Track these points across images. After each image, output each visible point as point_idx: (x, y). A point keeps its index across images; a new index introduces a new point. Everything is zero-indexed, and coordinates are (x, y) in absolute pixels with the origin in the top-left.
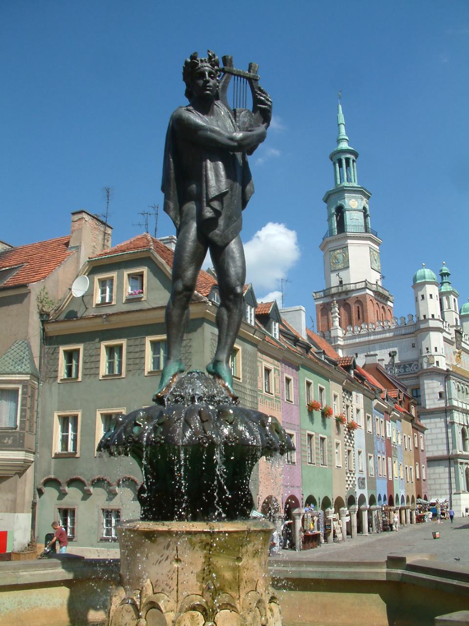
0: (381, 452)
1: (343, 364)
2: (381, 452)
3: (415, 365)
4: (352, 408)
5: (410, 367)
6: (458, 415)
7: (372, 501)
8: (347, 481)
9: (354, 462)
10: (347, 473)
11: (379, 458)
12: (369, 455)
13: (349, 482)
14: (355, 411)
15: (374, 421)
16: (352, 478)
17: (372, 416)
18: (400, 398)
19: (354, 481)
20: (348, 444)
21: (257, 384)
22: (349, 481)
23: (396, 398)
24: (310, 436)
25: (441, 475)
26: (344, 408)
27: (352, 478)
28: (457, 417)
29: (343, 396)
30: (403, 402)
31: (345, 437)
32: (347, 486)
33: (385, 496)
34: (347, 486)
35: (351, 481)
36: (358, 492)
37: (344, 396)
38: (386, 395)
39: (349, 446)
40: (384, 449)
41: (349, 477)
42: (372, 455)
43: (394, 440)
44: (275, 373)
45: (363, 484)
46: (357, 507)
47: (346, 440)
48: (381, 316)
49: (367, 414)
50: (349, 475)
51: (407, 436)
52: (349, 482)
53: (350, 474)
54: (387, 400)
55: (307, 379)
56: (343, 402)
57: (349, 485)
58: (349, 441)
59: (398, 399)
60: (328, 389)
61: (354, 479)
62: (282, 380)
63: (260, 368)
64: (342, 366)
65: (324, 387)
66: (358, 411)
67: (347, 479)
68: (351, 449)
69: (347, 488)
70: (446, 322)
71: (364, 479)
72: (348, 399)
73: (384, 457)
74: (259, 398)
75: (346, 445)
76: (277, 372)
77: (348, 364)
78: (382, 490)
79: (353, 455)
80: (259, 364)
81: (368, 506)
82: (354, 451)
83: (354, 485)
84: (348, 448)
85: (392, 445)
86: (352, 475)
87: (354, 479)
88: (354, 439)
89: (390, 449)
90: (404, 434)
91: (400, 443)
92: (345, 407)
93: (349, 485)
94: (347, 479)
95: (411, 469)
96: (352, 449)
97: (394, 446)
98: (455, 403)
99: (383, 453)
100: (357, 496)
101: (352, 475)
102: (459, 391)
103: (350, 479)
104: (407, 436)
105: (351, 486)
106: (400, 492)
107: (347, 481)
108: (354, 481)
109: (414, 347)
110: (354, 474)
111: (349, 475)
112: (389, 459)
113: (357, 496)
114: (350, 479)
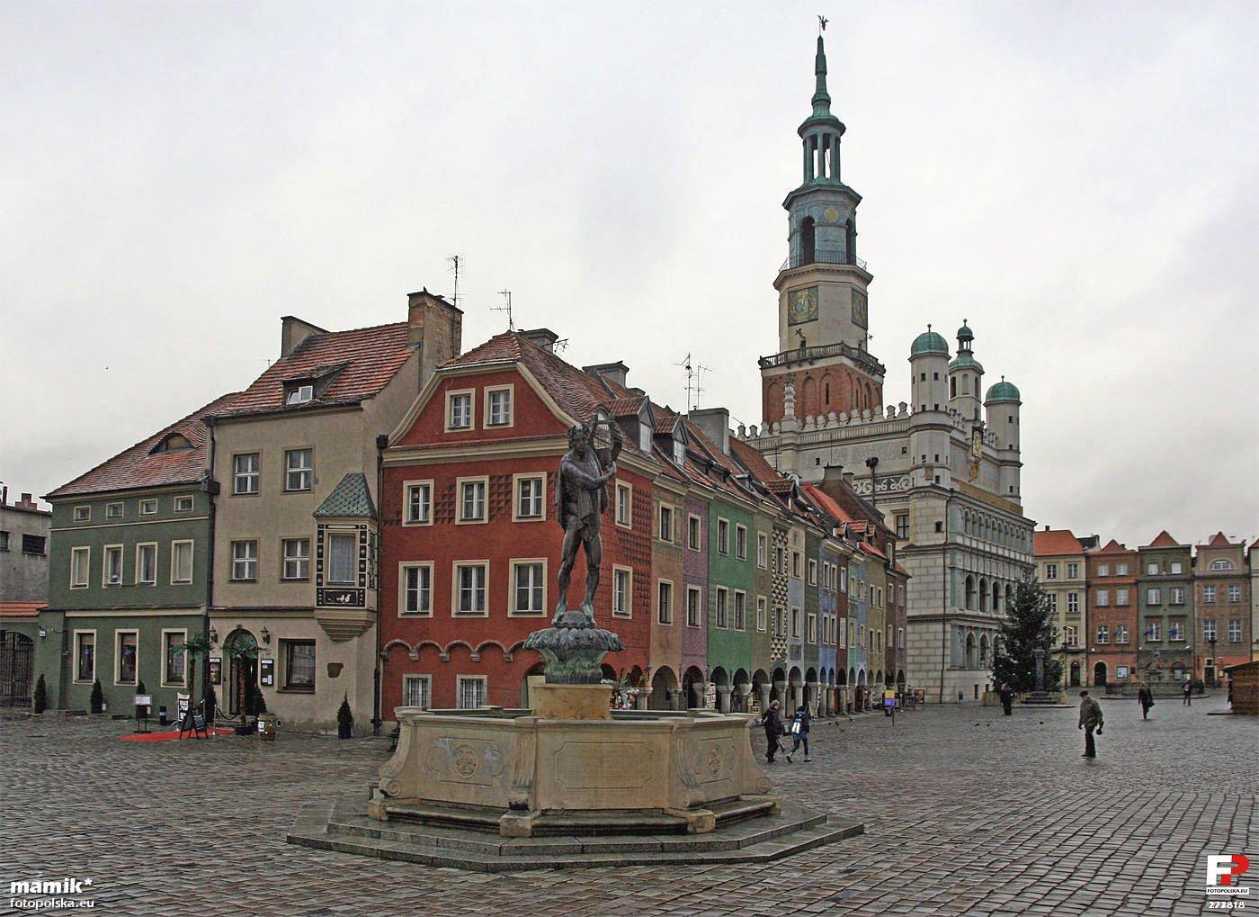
0: (830, 611)
6: (962, 558)
11: (826, 618)
17: (818, 562)
18: (868, 533)
23: (862, 534)
28: (960, 560)
42: (815, 615)
45: (798, 652)
46: (787, 683)
60: (753, 529)
70: (959, 415)
71: (799, 647)
73: (834, 617)
75: (774, 602)
84: (777, 606)
98: (959, 540)
99: (833, 612)
102: (967, 520)
112: (843, 621)
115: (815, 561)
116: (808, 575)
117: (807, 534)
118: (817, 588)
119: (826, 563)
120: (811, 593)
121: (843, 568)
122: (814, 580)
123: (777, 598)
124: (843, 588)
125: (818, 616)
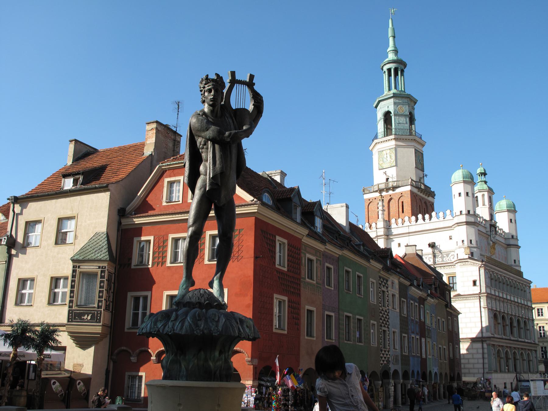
0: (415, 333)
1: (381, 255)
2: (415, 333)
3: (452, 255)
4: (388, 293)
5: (448, 256)
7: (406, 375)
8: (382, 357)
9: (389, 341)
10: (382, 351)
11: (413, 337)
12: (403, 335)
13: (383, 359)
14: (390, 296)
15: (409, 305)
16: (387, 355)
19: (389, 358)
20: (383, 325)
21: (300, 272)
22: (382, 356)
23: (431, 285)
24: (348, 317)
25: (472, 357)
26: (380, 293)
27: (387, 355)
29: (379, 283)
30: (438, 289)
31: (381, 319)
32: (382, 362)
33: (418, 372)
34: (382, 362)
35: (385, 358)
36: (392, 367)
37: (380, 283)
38: (421, 282)
39: (384, 326)
40: (418, 329)
41: (383, 354)
42: (406, 335)
44: (317, 263)
47: (381, 321)
48: (423, 210)
49: (402, 299)
50: (383, 352)
52: (383, 359)
53: (385, 351)
54: (423, 287)
55: (346, 268)
56: (380, 288)
57: (383, 361)
58: (384, 322)
59: (433, 286)
61: (388, 356)
62: (323, 268)
63: (303, 258)
64: (380, 256)
65: (362, 275)
66: (393, 296)
67: (382, 355)
68: (386, 329)
69: (382, 364)
72: (384, 286)
74: (302, 284)
75: (381, 326)
76: (319, 262)
77: (386, 254)
78: (414, 366)
79: (387, 334)
80: (302, 255)
81: (402, 381)
82: (388, 331)
83: (388, 361)
84: (383, 328)
86: (387, 352)
87: (388, 356)
88: (389, 320)
89: (423, 330)
90: (439, 318)
92: (382, 292)
93: (383, 361)
94: (382, 355)
96: (386, 329)
97: (428, 328)
100: (392, 371)
101: (387, 352)
103: (385, 356)
104: (441, 320)
105: (385, 362)
106: (434, 369)
107: (382, 357)
108: (389, 358)
109: (451, 239)
110: (388, 352)
111: (383, 352)
113: (392, 371)
114: (385, 356)
115: (405, 300)
116: (401, 309)
117: (400, 284)
118: (407, 318)
119: (412, 302)
120: (404, 322)
121: (422, 306)
122: (405, 312)
123: (383, 323)
124: (422, 318)
125: (408, 336)
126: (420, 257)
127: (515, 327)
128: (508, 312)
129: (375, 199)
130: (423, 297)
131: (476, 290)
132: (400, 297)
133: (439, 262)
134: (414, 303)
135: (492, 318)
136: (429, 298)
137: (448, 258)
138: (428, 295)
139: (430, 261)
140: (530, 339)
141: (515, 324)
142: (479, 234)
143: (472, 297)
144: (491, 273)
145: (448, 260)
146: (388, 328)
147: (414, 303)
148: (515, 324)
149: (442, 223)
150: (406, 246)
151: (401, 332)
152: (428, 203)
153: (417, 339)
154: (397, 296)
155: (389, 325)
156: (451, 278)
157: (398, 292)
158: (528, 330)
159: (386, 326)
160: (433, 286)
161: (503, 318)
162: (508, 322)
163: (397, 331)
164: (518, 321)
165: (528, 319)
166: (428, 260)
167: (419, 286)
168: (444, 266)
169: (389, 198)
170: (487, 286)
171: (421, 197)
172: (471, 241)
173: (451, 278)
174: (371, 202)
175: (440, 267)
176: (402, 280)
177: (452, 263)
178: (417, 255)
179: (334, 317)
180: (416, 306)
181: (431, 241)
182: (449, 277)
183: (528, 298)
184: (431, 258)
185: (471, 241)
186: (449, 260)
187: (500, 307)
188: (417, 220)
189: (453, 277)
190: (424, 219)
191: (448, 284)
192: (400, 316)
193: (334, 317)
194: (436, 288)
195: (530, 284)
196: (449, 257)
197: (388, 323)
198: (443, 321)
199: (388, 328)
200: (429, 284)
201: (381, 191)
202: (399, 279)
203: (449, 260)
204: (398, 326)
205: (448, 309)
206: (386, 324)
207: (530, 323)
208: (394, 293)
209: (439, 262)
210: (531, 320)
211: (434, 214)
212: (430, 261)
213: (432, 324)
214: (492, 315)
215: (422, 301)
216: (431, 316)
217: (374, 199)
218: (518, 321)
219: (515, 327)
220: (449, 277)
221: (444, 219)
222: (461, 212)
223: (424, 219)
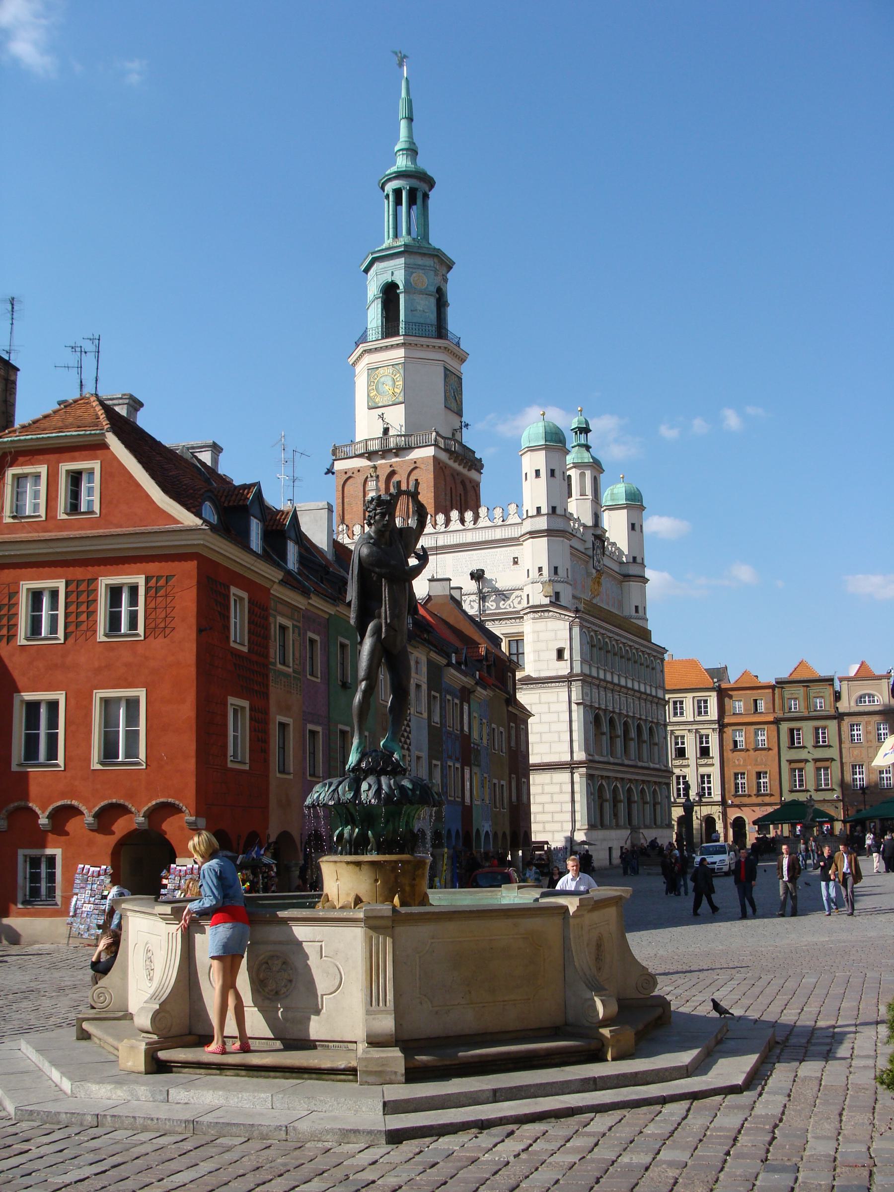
43: (475, 735)
51: (498, 729)
54: (466, 666)
59: (484, 663)
85: (472, 745)
91: (485, 741)
95: (502, 785)
97: (476, 747)
104: (498, 729)
124: (466, 728)
126: (458, 604)
127: (632, 739)
128: (620, 710)
129: (359, 471)
130: (469, 687)
131: (563, 669)
132: (429, 689)
133: (491, 610)
134: (453, 700)
135: (591, 723)
136: (479, 689)
137: (509, 602)
138: (477, 684)
139: (472, 607)
140: (659, 763)
141: (633, 734)
142: (571, 554)
143: (559, 682)
144: (592, 633)
145: (508, 607)
146: (408, 749)
147: (453, 700)
148: (633, 734)
149: (498, 530)
150: (430, 580)
151: (431, 757)
152: (468, 483)
153: (457, 768)
154: (424, 687)
155: (410, 745)
156: (514, 645)
157: (425, 680)
158: (656, 744)
159: (406, 746)
160: (484, 663)
161: (612, 721)
162: (620, 731)
163: (424, 754)
164: (639, 727)
165: (657, 724)
166: (471, 607)
167: (459, 663)
168: (501, 620)
169: (389, 471)
170: (583, 661)
171: (454, 470)
172: (556, 568)
173: (514, 645)
174: (350, 477)
175: (493, 620)
176: (433, 655)
177: (518, 612)
178: (452, 598)
179: (321, 734)
180: (456, 704)
181: (475, 567)
182: (509, 641)
183: (658, 682)
184: (474, 601)
185: (556, 568)
186: (510, 607)
187: (606, 700)
188: (448, 521)
189: (517, 640)
190: (462, 521)
191: (508, 654)
192: (429, 725)
193: (321, 734)
194: (489, 667)
195: (663, 654)
196: (511, 600)
197: (408, 741)
198: (501, 732)
199: (408, 749)
200: (477, 658)
201: (370, 455)
202: (428, 654)
203: (510, 607)
204: (425, 747)
205: (510, 709)
206: (405, 743)
207: (660, 730)
208: (419, 683)
209: (491, 610)
210: (661, 724)
211: (483, 511)
212: (472, 607)
213: (481, 739)
214: (591, 718)
215: (465, 694)
216: (481, 724)
217: (356, 472)
218: (639, 727)
219: (632, 739)
220: (509, 641)
221: (503, 521)
222: (539, 509)
223: (462, 521)
